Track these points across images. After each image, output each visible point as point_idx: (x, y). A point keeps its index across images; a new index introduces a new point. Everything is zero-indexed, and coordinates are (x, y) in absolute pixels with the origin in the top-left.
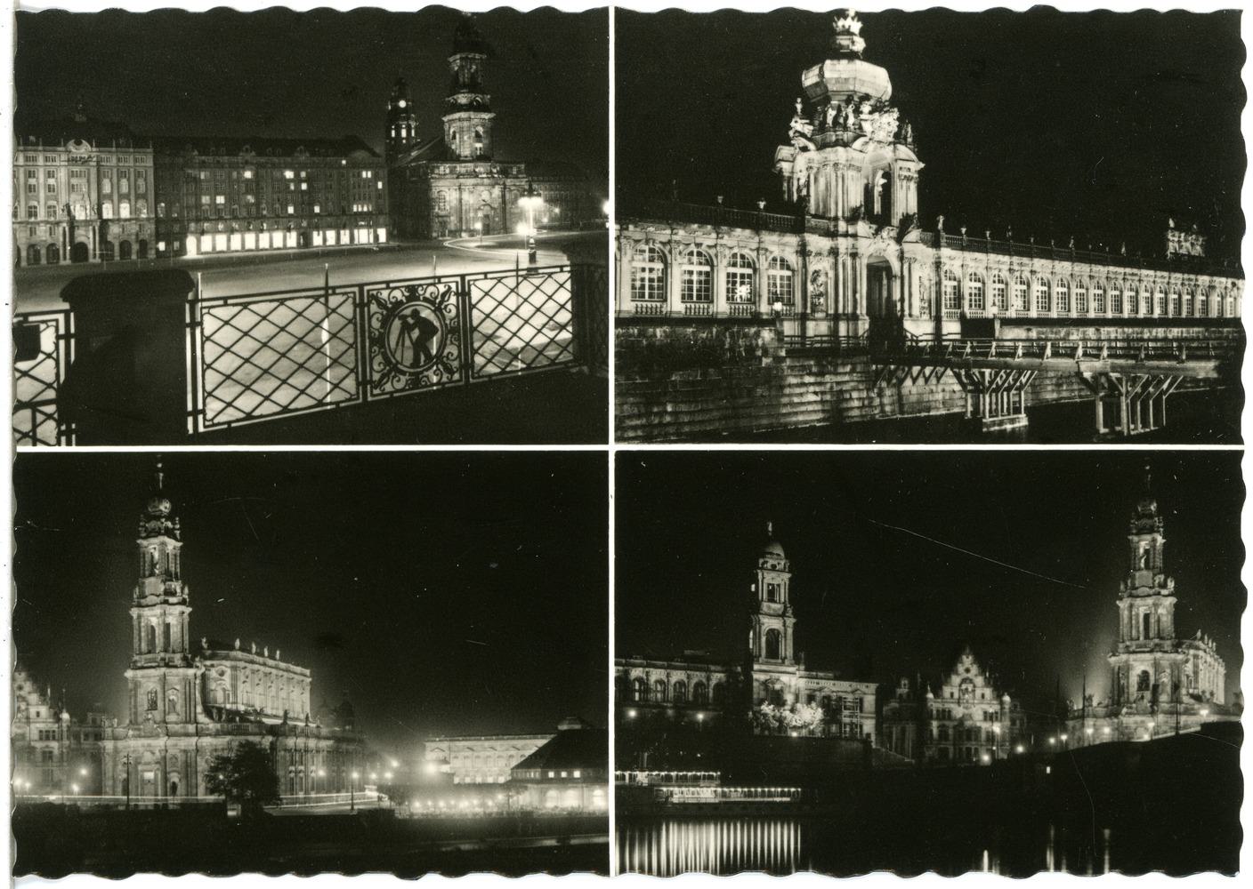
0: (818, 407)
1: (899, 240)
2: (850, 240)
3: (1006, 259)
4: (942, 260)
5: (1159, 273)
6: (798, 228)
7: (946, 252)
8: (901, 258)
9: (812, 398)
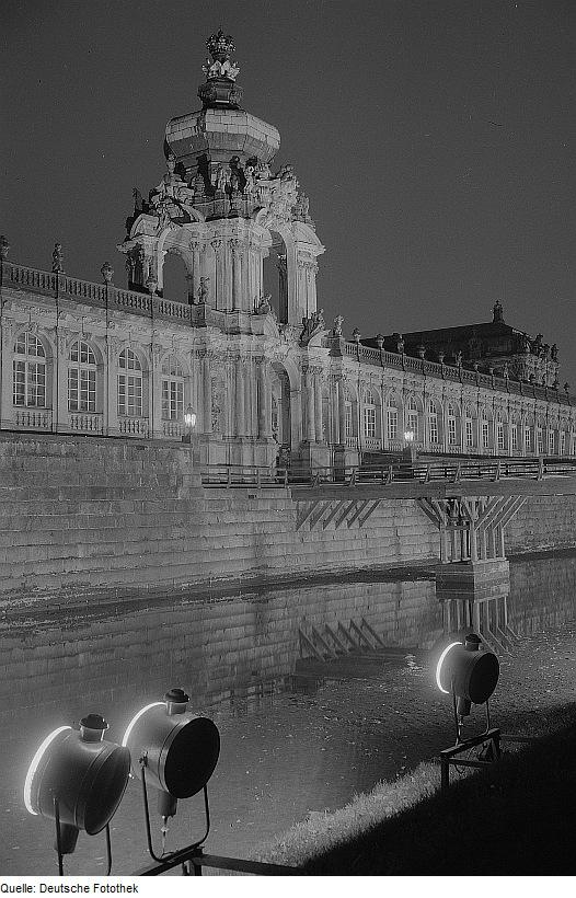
0: (243, 555)
1: (303, 344)
3: (399, 375)
5: (539, 403)
6: (200, 323)
8: (305, 369)
9: (238, 543)
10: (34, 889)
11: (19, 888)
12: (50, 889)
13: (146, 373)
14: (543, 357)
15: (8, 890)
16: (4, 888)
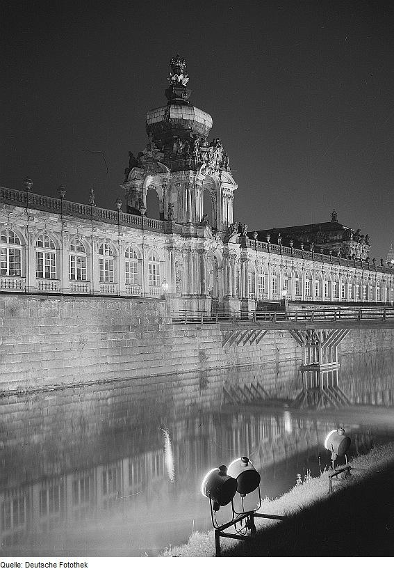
2: (199, 241)
4: (248, 257)
5: (358, 270)
7: (250, 251)
10: (22, 566)
11: (12, 564)
12: (32, 565)
13: (140, 260)
14: (360, 242)
15: (5, 566)
16: (3, 565)
